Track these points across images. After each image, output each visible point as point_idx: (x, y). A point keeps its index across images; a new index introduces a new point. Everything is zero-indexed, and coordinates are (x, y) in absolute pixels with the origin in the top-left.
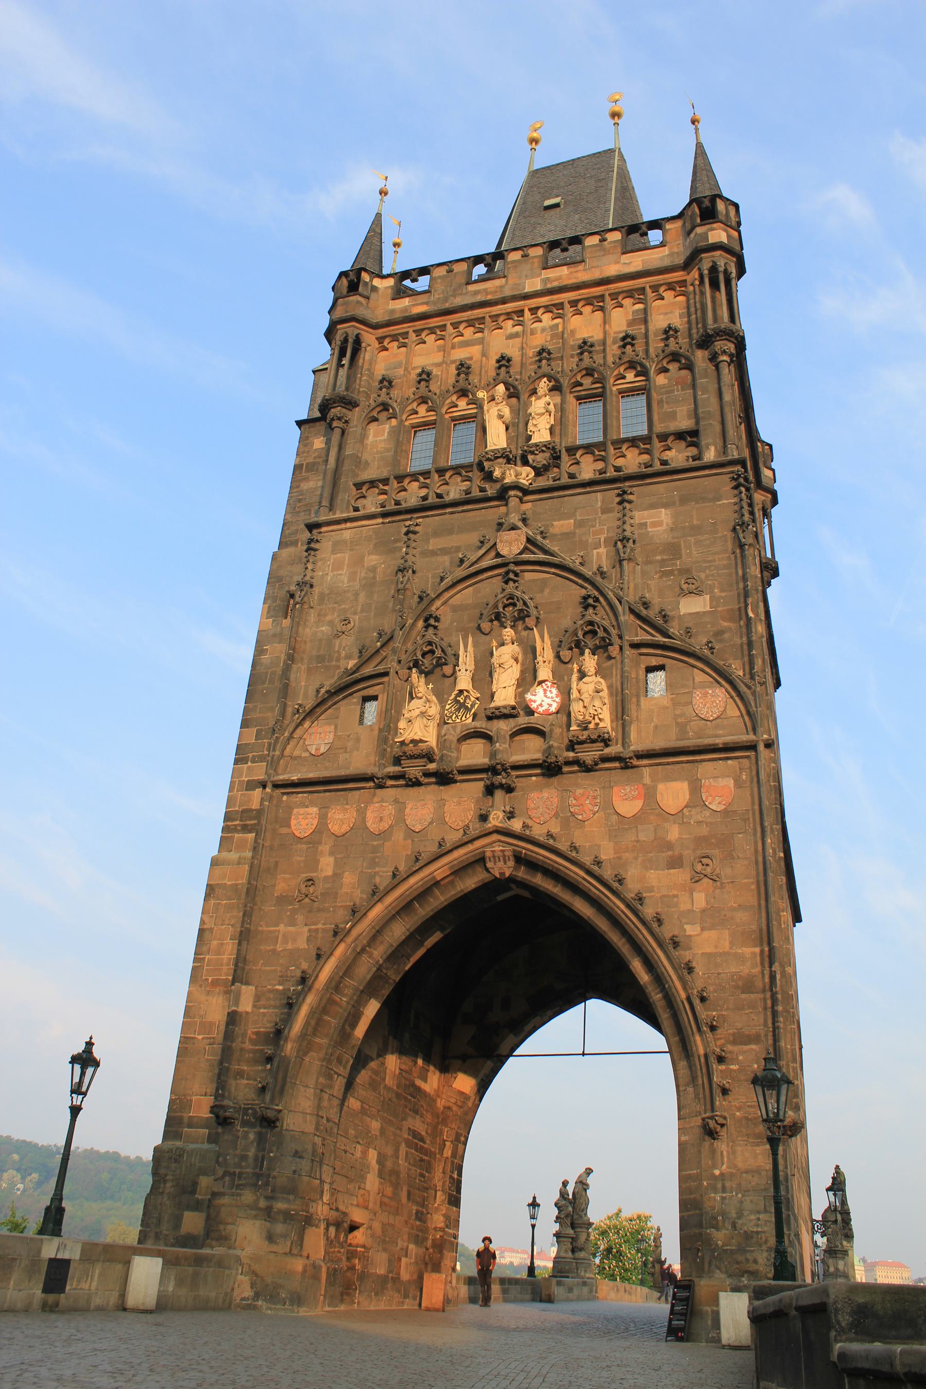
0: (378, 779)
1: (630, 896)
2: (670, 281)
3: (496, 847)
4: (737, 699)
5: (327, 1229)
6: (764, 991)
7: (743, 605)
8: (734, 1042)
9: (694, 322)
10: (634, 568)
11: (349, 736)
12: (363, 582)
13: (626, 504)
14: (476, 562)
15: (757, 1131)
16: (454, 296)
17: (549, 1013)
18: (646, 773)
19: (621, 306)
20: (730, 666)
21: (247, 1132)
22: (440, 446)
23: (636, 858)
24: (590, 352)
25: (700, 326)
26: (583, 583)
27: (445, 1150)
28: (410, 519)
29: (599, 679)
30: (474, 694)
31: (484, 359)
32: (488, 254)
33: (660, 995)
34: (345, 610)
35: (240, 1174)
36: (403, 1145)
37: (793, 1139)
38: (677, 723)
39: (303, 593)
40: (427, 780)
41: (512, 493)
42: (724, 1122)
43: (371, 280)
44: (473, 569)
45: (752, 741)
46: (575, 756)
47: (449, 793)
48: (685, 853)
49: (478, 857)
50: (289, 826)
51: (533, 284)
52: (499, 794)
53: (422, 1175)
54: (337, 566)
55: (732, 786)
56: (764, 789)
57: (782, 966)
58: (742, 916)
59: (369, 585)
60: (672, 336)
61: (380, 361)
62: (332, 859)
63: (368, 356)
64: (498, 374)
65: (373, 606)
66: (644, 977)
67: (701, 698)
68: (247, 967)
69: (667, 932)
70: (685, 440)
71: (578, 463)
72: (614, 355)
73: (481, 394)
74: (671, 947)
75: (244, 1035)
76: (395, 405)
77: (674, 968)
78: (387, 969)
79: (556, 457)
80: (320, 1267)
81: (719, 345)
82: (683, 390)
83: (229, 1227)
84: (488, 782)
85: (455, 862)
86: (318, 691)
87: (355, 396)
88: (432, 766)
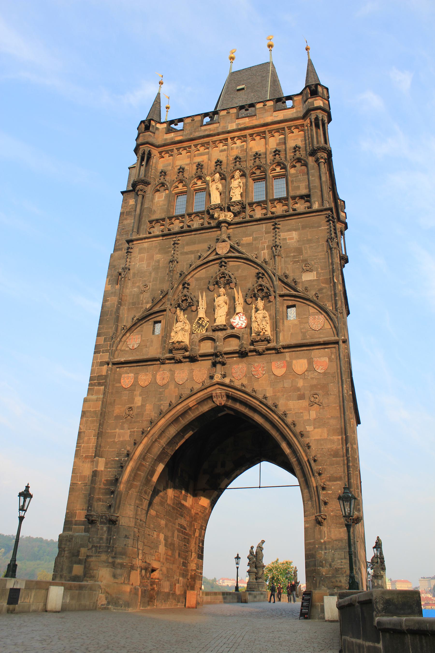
0: (162, 360)
1: (280, 413)
2: (296, 124)
3: (217, 391)
4: (329, 320)
5: (141, 571)
6: (343, 456)
7: (331, 276)
8: (330, 480)
9: (308, 143)
10: (281, 259)
11: (148, 340)
12: (154, 267)
13: (276, 229)
14: (206, 257)
15: (341, 521)
16: (195, 132)
17: (244, 468)
18: (287, 355)
19: (274, 136)
20: (326, 305)
21: (103, 527)
22: (189, 203)
23: (283, 395)
24: (259, 158)
25: (310, 145)
26: (257, 267)
27: (196, 533)
28: (175, 237)
29: (265, 311)
30: (206, 319)
31: (209, 161)
32: (210, 112)
33: (295, 459)
34: (145, 281)
35: (100, 547)
36: (176, 531)
37: (357, 525)
38: (302, 332)
39: (125, 273)
40: (185, 360)
41: (223, 225)
42: (325, 517)
43: (156, 125)
44: (205, 261)
45: (336, 340)
46: (254, 348)
47: (195, 366)
48: (306, 392)
49: (209, 396)
50: (120, 383)
51: (232, 126)
52: (219, 366)
53: (185, 545)
54: (141, 260)
55: (327, 361)
56: (342, 362)
57: (352, 444)
58: (333, 422)
59: (156, 269)
60: (298, 150)
61: (160, 163)
62: (140, 398)
63: (154, 161)
64: (216, 169)
65: (158, 279)
66: (287, 451)
67: (312, 320)
68: (101, 450)
69: (298, 430)
70: (304, 199)
71: (254, 210)
72: (270, 159)
73: (208, 178)
74: (300, 437)
75: (100, 481)
76: (167, 184)
77: (301, 446)
78: (167, 449)
79: (244, 208)
80: (138, 589)
81: (319, 154)
82: (303, 175)
83: (95, 571)
84: (213, 361)
85: (199, 398)
86: (133, 319)
87: (149, 180)
88: (187, 354)
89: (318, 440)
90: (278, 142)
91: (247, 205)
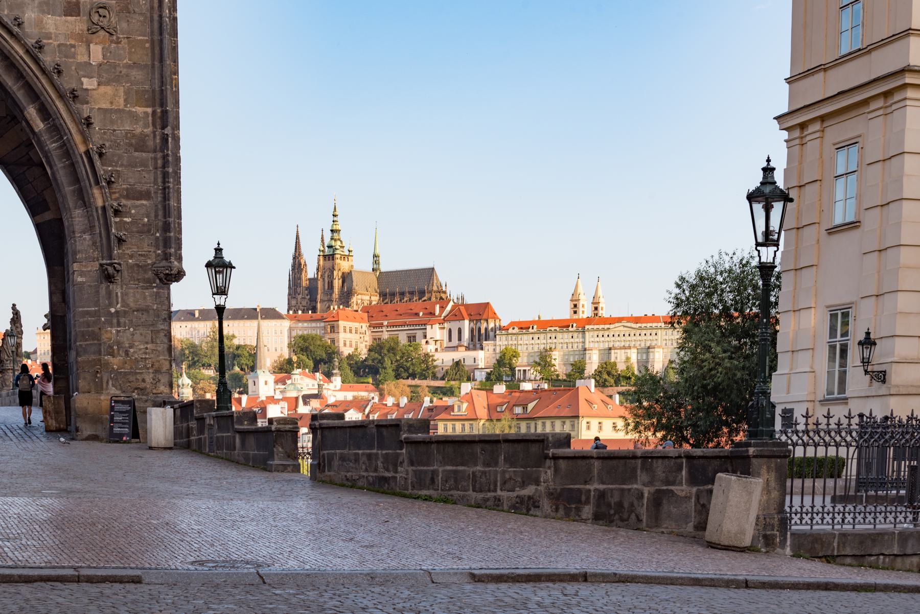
6: (155, 151)
8: (128, 197)
58: (137, 75)
89: (105, 111)
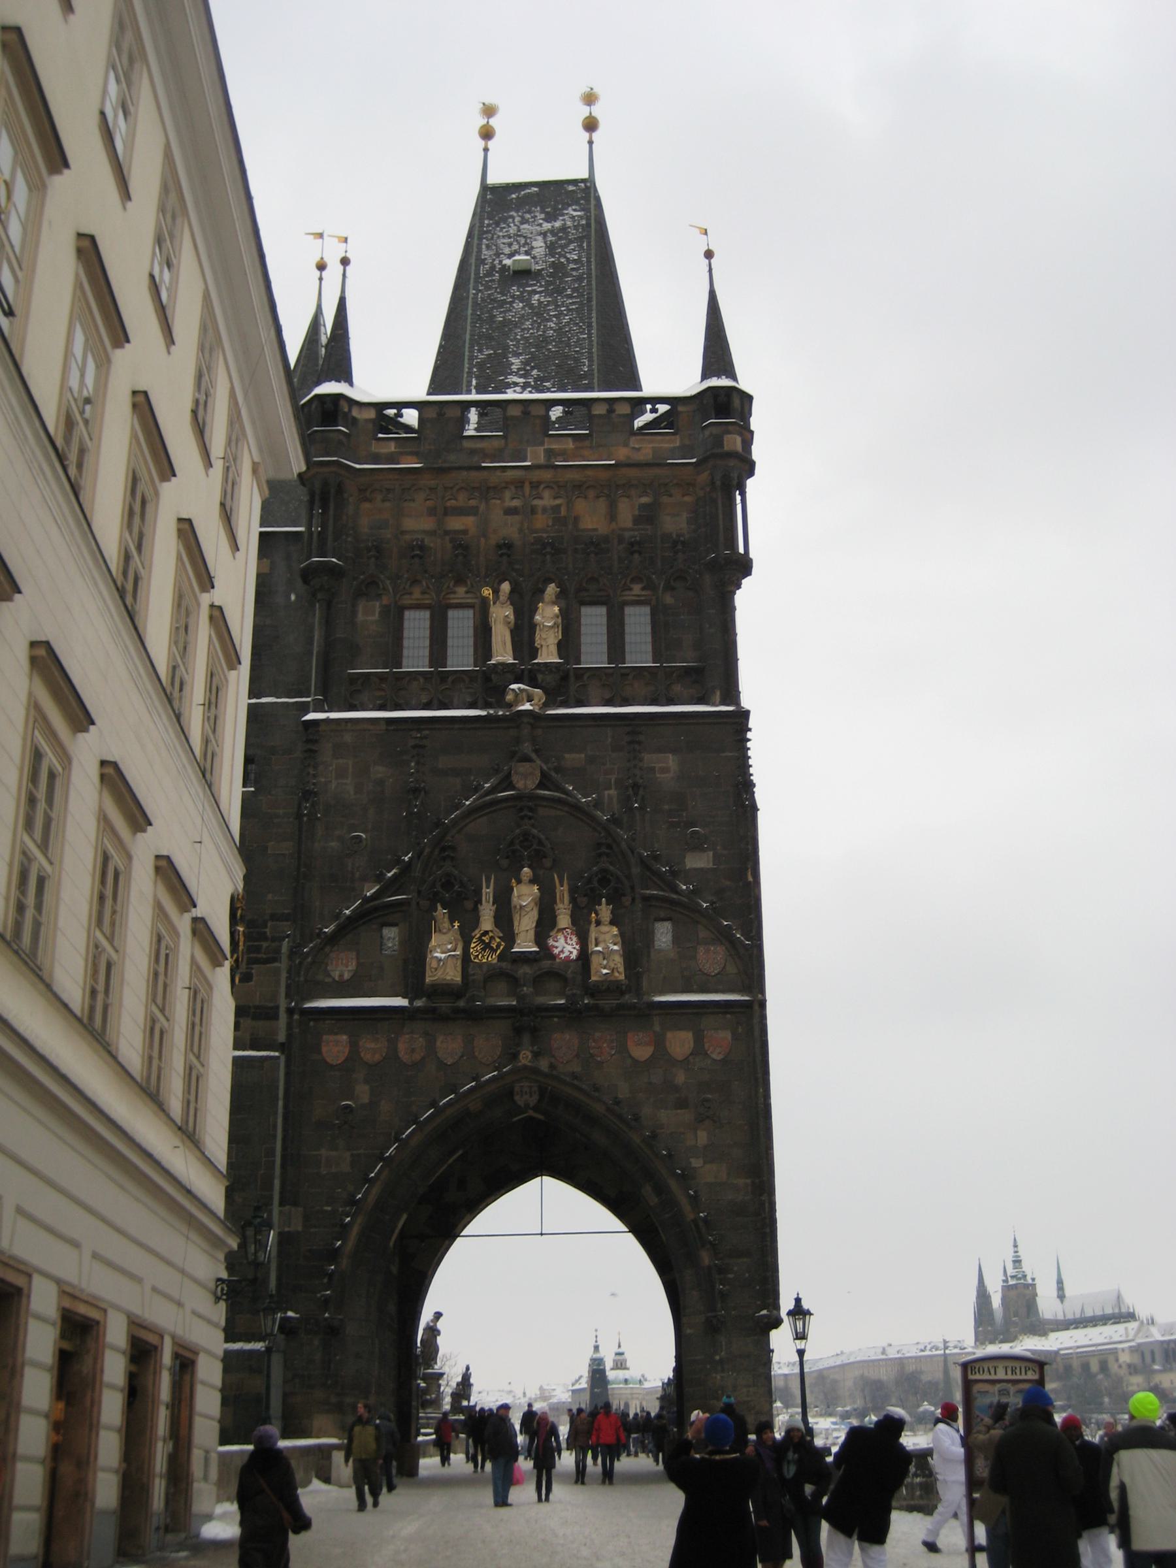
29: (615, 930)
31: (483, 540)
41: (525, 720)
43: (350, 410)
50: (320, 1053)
62: (367, 1088)
66: (653, 1200)
73: (487, 592)
79: (565, 678)
88: (461, 1003)
90: (637, 513)
91: (571, 673)
